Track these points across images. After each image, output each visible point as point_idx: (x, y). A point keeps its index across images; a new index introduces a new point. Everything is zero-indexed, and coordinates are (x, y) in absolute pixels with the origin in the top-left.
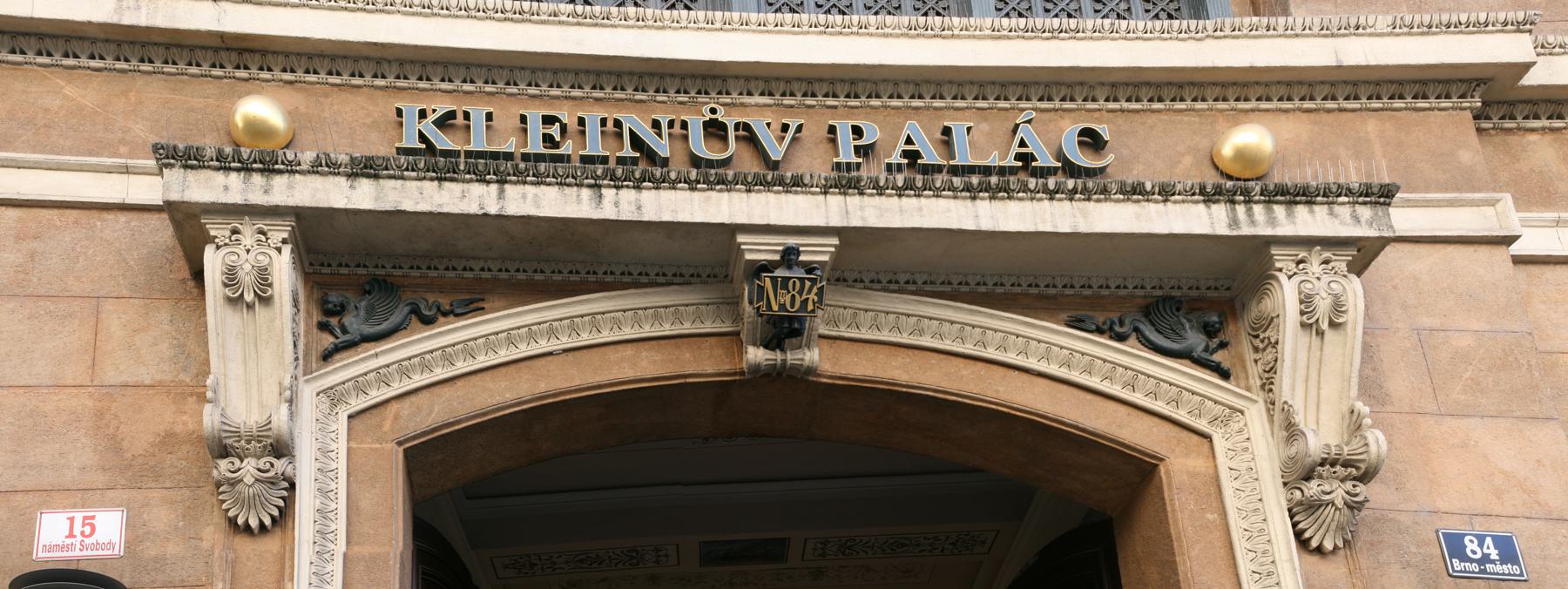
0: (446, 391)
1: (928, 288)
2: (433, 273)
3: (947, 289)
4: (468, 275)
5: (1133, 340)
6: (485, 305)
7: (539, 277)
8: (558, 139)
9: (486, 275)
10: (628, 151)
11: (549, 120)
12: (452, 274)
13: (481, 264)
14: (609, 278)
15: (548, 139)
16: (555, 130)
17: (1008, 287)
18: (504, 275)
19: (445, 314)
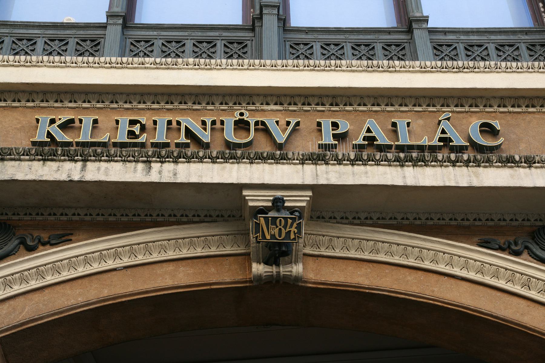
0: (36, 297)
1: (380, 222)
2: (39, 218)
3: (394, 222)
4: (64, 218)
5: (525, 255)
6: (73, 238)
7: (112, 219)
8: (137, 133)
9: (76, 218)
10: (183, 139)
11: (133, 123)
12: (52, 218)
13: (73, 211)
14: (160, 219)
15: (131, 134)
16: (137, 129)
17: (436, 221)
18: (88, 218)
19: (44, 244)
